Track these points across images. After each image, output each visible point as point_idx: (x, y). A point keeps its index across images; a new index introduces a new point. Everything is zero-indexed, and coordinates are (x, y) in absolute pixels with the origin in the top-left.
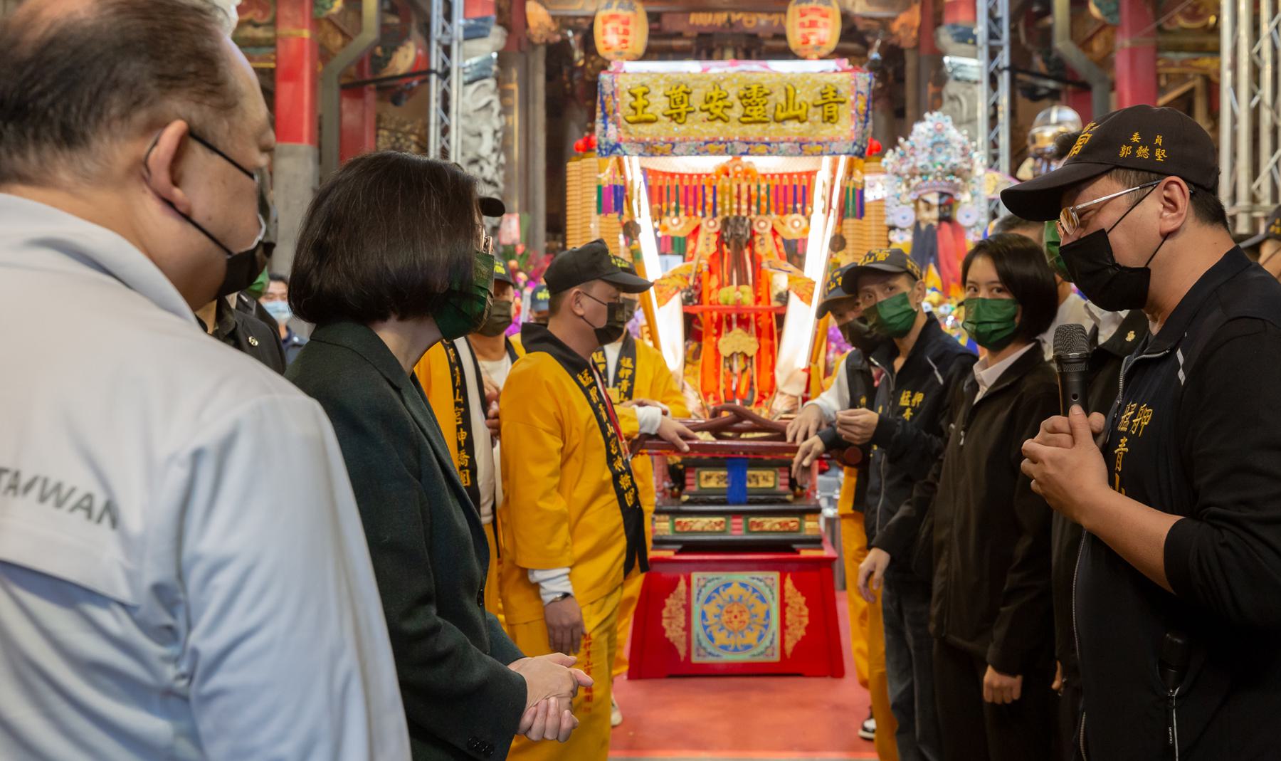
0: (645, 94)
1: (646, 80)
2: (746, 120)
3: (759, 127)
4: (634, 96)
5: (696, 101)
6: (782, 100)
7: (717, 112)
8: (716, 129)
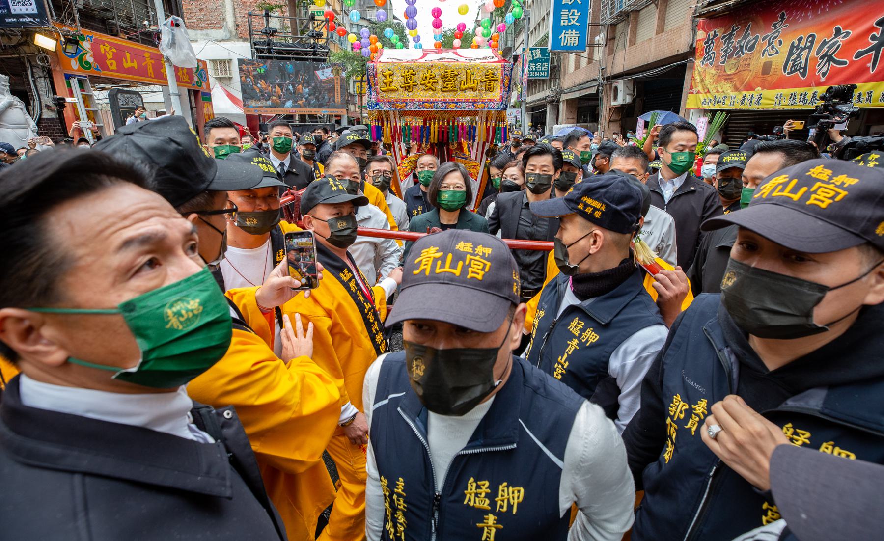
0: (391, 75)
1: (390, 66)
2: (444, 90)
3: (453, 93)
4: (385, 77)
5: (418, 79)
6: (464, 78)
7: (429, 85)
8: (428, 95)
